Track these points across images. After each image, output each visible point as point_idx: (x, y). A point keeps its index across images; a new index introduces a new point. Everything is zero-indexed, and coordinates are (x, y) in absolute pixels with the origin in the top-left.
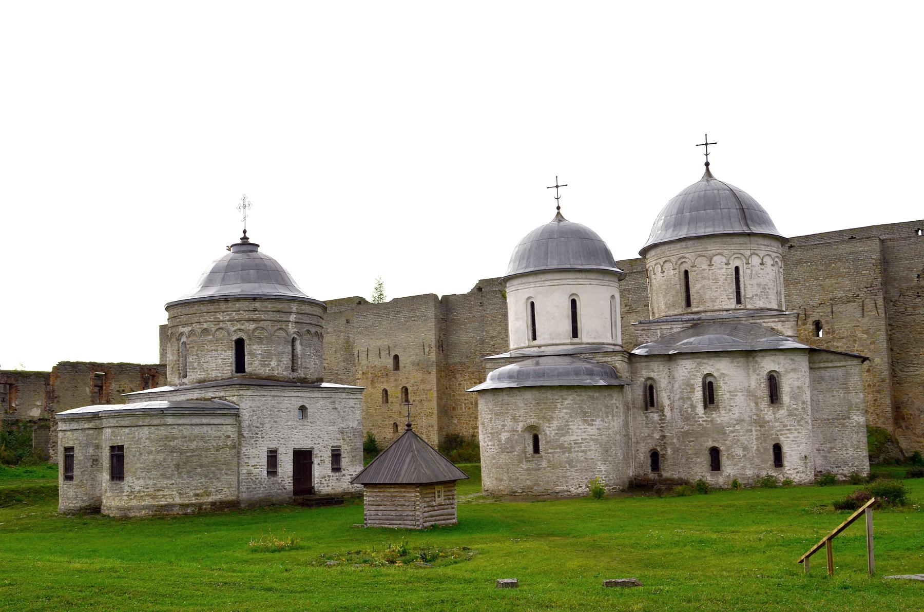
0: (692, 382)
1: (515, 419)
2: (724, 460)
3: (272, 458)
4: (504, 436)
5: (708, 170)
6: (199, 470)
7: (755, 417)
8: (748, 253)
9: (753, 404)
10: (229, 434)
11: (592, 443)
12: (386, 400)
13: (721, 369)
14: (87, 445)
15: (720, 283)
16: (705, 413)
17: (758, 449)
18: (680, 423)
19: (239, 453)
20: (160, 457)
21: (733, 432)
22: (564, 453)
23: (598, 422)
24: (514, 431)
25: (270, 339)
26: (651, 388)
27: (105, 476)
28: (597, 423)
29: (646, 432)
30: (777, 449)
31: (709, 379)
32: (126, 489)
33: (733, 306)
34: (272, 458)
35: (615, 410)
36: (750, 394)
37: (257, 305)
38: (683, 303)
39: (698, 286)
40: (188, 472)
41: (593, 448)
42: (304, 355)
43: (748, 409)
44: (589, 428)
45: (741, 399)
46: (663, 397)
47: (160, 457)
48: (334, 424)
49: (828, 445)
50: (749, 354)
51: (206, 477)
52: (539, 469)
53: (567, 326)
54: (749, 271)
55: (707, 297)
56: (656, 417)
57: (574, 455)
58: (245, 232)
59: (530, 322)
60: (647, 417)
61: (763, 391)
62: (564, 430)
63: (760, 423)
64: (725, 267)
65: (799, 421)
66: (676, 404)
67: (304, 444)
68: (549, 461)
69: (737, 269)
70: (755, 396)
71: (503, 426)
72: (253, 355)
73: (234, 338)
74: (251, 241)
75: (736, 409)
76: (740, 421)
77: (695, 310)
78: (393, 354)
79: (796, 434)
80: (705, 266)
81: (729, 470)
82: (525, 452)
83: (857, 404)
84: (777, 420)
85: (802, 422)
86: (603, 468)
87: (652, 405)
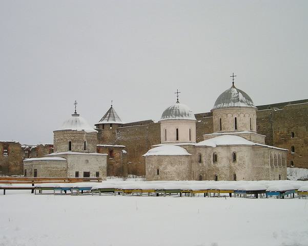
3: (77, 174)
4: (150, 169)
8: (239, 113)
18: (207, 167)
23: (176, 166)
24: (152, 168)
29: (198, 170)
34: (77, 174)
36: (228, 158)
42: (88, 146)
46: (203, 159)
48: (97, 165)
50: (228, 146)
56: (200, 164)
61: (231, 158)
62: (165, 168)
63: (230, 167)
69: (236, 118)
73: (68, 141)
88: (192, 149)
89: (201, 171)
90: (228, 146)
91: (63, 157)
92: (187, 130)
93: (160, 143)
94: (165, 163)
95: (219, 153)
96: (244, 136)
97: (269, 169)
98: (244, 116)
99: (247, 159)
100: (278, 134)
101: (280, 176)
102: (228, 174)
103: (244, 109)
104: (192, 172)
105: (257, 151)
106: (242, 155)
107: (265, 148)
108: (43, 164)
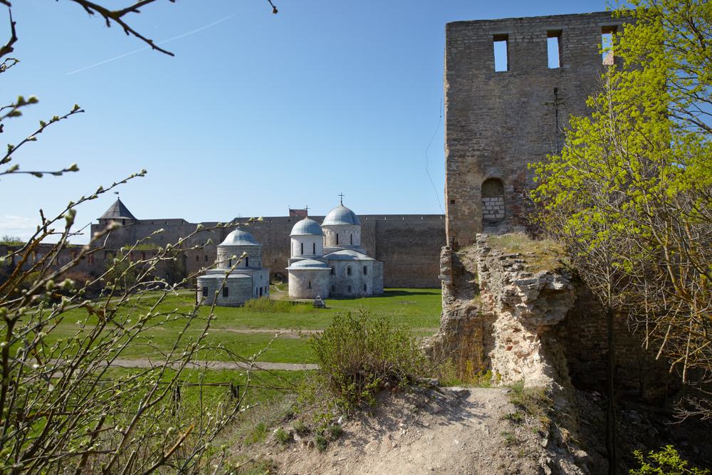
1: (305, 278)
12: (198, 260)
30: (365, 285)
36: (359, 271)
45: (357, 272)
46: (336, 271)
56: (334, 276)
61: (363, 270)
62: (318, 281)
63: (361, 279)
81: (353, 292)
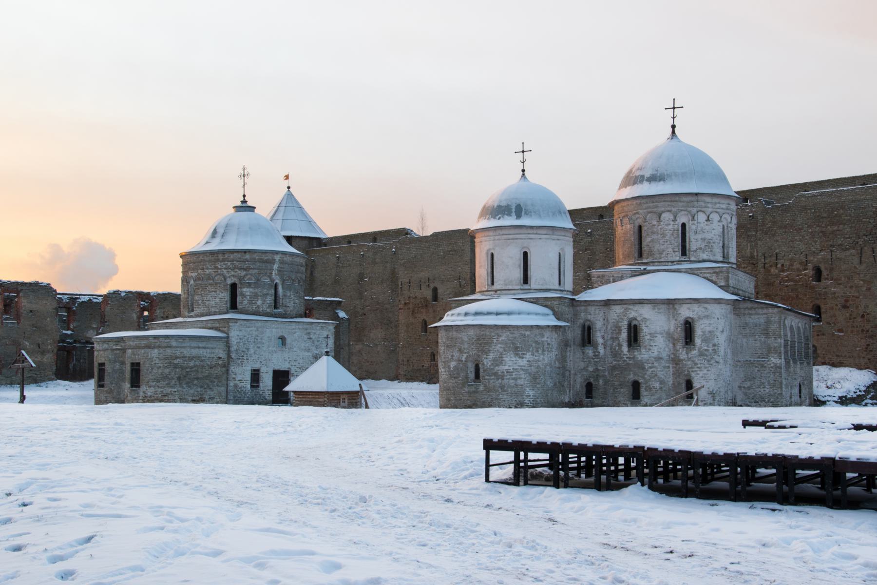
0: (620, 324)
2: (643, 390)
3: (256, 376)
4: (453, 365)
5: (673, 132)
6: (196, 382)
7: (672, 356)
8: (695, 210)
9: (671, 345)
10: (221, 356)
11: (522, 372)
13: (645, 312)
14: (115, 362)
15: (667, 238)
16: (629, 351)
17: (673, 384)
18: (611, 360)
19: (228, 370)
20: (167, 371)
21: (651, 368)
22: (498, 379)
23: (528, 356)
25: (257, 284)
26: (589, 328)
27: (127, 385)
28: (527, 356)
29: (582, 365)
30: (689, 385)
31: (634, 323)
32: (141, 394)
33: (678, 258)
34: (256, 376)
35: (546, 346)
36: (669, 336)
37: (248, 256)
38: (636, 255)
39: (649, 239)
40: (187, 383)
41: (523, 376)
42: (284, 295)
43: (667, 349)
44: (520, 360)
46: (599, 337)
47: (167, 371)
48: (309, 350)
49: (749, 384)
51: (201, 387)
52: (476, 392)
53: (518, 274)
54: (694, 227)
55: (656, 249)
56: (590, 352)
57: (505, 381)
58: (244, 196)
59: (490, 270)
60: (583, 353)
61: (680, 334)
62: (499, 361)
63: (676, 361)
64: (672, 223)
65: (708, 361)
66: (609, 342)
67: (283, 367)
68: (485, 386)
69: (684, 225)
70: (673, 339)
71: (452, 356)
72: (243, 295)
73: (229, 282)
74: (249, 204)
75: (655, 348)
76: (659, 359)
77: (645, 261)
78: (432, 286)
79: (705, 372)
80: (655, 222)
82: (467, 378)
83: (775, 348)
84: (689, 359)
85: (713, 362)
86: (531, 393)
87: (589, 342)
88: (566, 306)
89: (591, 369)
90: (671, 303)
91: (217, 329)
92: (552, 259)
93: (473, 291)
94: (499, 347)
95: (645, 320)
96: (711, 277)
97: (780, 368)
98: (708, 220)
99: (722, 339)
100: (773, 271)
101: (800, 386)
102: (670, 381)
103: (708, 199)
104: (567, 373)
105: (748, 319)
106: (710, 329)
107: (770, 310)
108: (159, 347)
